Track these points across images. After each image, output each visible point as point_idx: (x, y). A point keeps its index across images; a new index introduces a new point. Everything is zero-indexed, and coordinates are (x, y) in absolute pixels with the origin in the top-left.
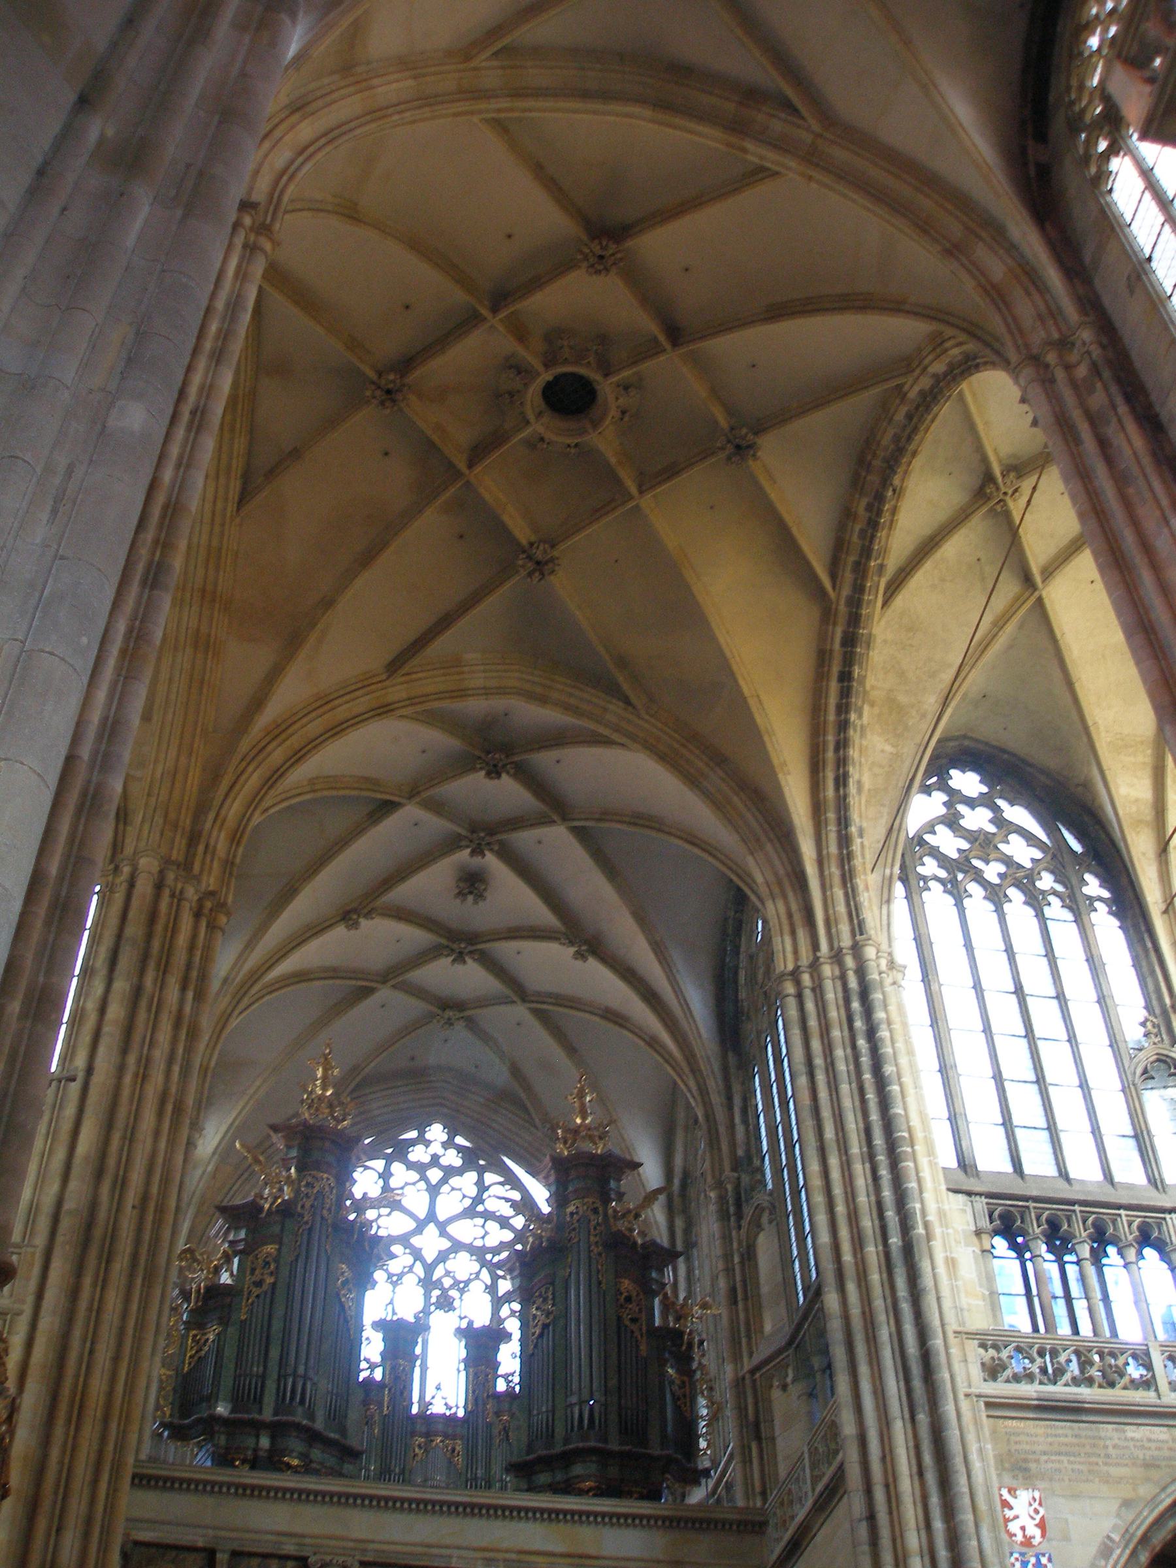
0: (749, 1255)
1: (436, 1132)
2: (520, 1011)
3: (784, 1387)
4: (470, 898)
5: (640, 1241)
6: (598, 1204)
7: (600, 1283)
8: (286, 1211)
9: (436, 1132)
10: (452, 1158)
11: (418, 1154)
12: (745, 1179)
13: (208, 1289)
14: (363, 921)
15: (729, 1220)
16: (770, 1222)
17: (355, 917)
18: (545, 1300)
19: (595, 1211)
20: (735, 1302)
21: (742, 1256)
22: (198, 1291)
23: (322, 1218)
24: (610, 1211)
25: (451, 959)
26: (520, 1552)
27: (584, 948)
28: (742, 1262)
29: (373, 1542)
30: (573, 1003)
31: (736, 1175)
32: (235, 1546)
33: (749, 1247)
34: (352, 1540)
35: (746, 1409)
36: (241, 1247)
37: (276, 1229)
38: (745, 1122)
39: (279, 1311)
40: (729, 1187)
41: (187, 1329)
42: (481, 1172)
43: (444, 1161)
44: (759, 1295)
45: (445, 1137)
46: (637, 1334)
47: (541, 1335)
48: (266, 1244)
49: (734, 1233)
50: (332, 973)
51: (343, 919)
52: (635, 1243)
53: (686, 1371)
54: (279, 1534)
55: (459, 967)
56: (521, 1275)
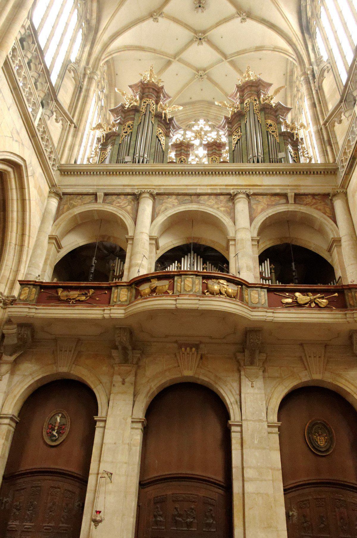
0: (320, 88)
1: (202, 122)
2: (226, 66)
3: (340, 122)
4: (200, 10)
5: (274, 105)
6: (256, 98)
7: (259, 121)
8: (135, 110)
9: (202, 122)
10: (207, 128)
11: (195, 128)
12: (315, 68)
13: (107, 135)
14: (160, 19)
15: (310, 83)
16: (328, 72)
17: (155, 14)
18: (238, 132)
19: (255, 100)
20: (315, 107)
21: (317, 91)
22: (103, 137)
23: (150, 112)
24: (261, 99)
25: (197, 43)
26: (226, 186)
27: (244, 14)
28: (317, 93)
29: (164, 186)
30: (244, 52)
31: (311, 67)
32: (106, 191)
33: (319, 87)
34: (155, 186)
35: (323, 138)
36: (118, 121)
37: (133, 116)
38: (315, 53)
39: (134, 138)
40: (309, 72)
41: (101, 151)
42: (218, 131)
43: (204, 129)
44: (325, 100)
45: (205, 122)
46: (275, 136)
47: (237, 143)
48: (128, 121)
49: (312, 85)
50: (154, 51)
51: (152, 16)
52: (272, 105)
53: (296, 150)
54: (124, 186)
55: (200, 46)
56: (228, 127)
